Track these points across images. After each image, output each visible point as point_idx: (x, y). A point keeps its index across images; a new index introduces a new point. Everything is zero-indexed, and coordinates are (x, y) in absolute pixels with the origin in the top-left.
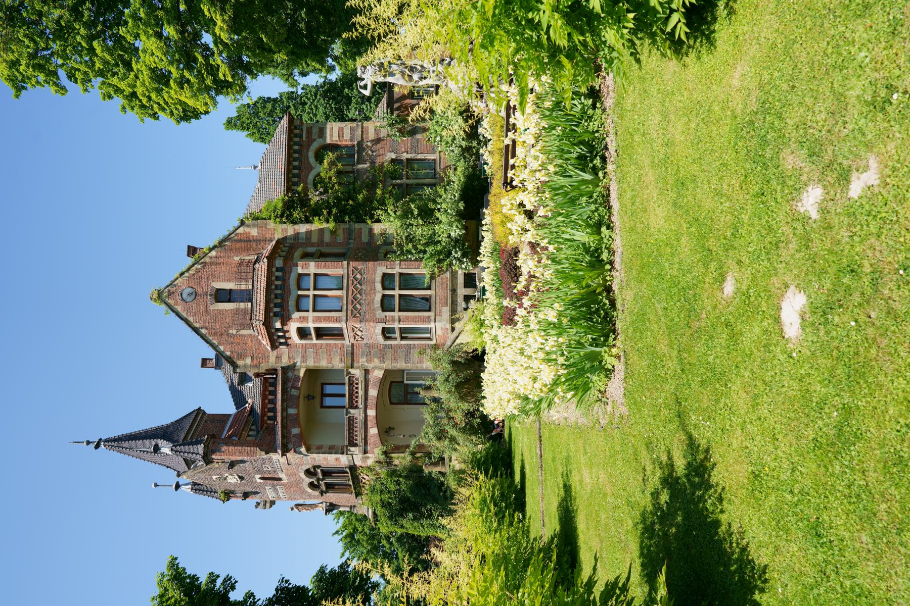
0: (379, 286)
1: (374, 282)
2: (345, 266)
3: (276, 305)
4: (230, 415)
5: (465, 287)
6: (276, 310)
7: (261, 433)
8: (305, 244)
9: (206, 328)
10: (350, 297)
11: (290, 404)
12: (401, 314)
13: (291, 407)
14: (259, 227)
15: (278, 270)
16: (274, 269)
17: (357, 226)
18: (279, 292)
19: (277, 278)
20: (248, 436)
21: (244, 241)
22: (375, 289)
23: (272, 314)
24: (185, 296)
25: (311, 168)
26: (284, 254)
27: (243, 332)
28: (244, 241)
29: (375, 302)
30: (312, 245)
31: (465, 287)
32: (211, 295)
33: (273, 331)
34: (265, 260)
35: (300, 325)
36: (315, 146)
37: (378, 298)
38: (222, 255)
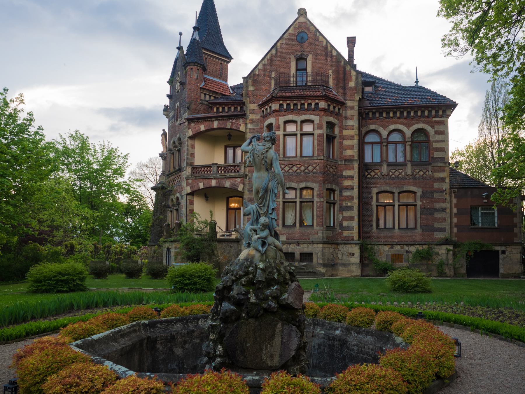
0: (303, 185)
1: (306, 181)
2: (319, 158)
3: (288, 105)
4: (226, 81)
5: (301, 253)
6: (285, 105)
7: (206, 103)
8: (342, 125)
9: (276, 54)
10: (294, 162)
11: (220, 122)
12: (281, 203)
13: (219, 123)
14: (355, 88)
15: (317, 104)
16: (317, 101)
17: (356, 166)
18: (299, 107)
19: (310, 104)
20: (205, 94)
21: (344, 77)
22: (301, 182)
23: (281, 102)
24: (301, 34)
25: (408, 127)
26: (331, 108)
27: (273, 82)
28: (344, 77)
29: (291, 183)
30: (341, 131)
31: (301, 253)
32: (302, 54)
33: (270, 105)
34: (324, 93)
35: (274, 125)
36: (428, 128)
37: (294, 185)
38: (334, 60)
